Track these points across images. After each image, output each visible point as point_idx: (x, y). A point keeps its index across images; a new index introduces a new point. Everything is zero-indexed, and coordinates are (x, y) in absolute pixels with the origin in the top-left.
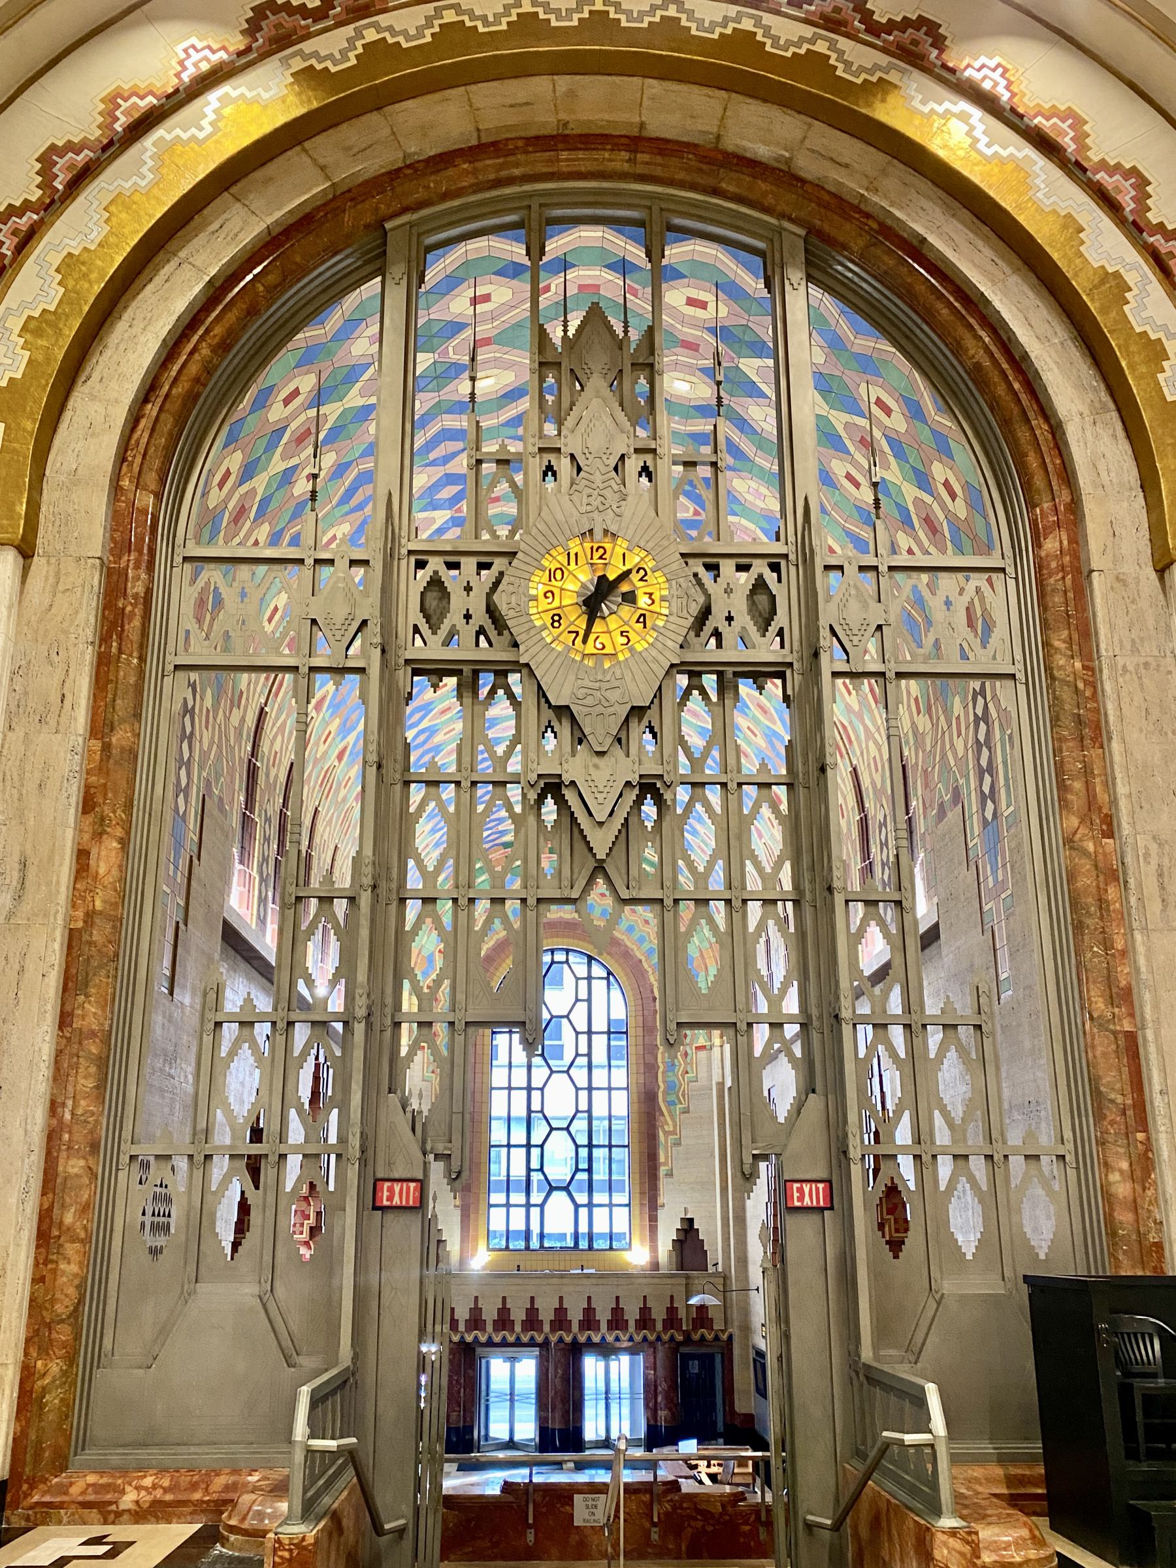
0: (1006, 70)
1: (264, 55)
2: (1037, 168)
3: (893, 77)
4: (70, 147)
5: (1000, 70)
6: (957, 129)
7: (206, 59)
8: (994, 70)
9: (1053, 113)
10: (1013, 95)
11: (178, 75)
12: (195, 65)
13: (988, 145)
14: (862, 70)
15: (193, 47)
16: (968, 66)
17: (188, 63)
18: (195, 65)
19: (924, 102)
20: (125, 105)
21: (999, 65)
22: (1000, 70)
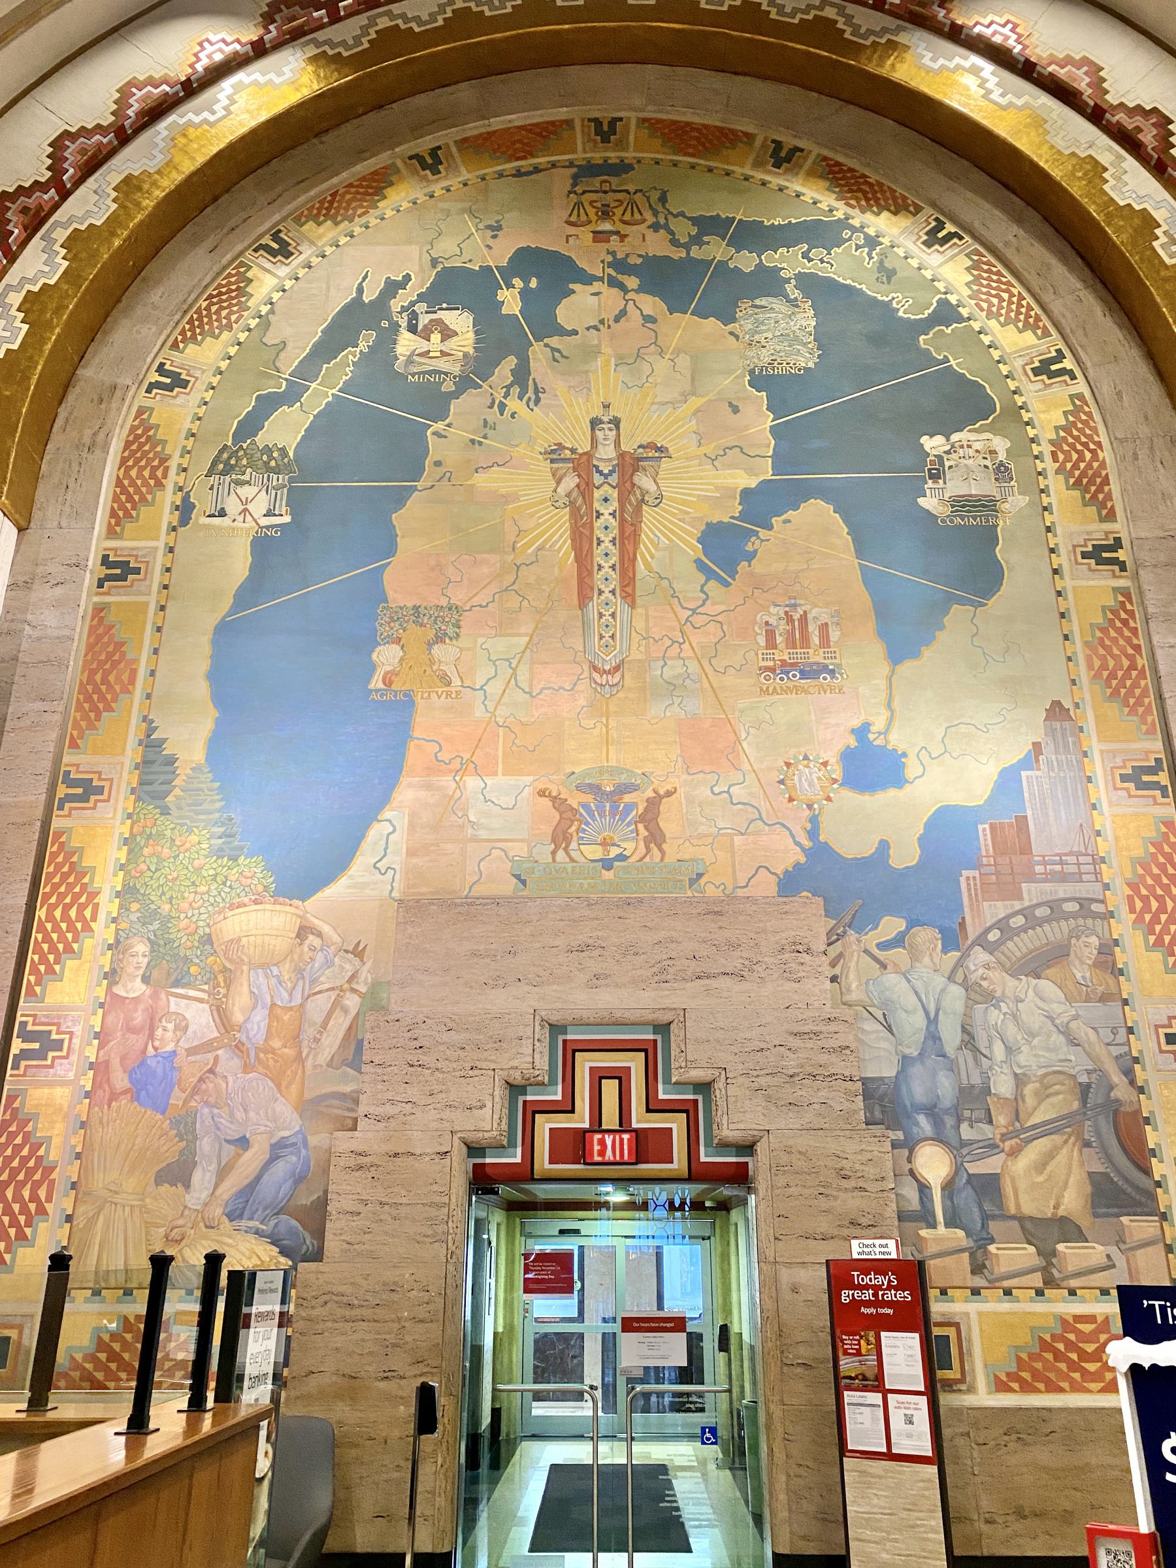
0: (1015, 26)
1: (278, 46)
2: (1054, 115)
3: (902, 38)
4: (83, 132)
5: (1010, 26)
6: (970, 81)
7: (221, 50)
8: (1004, 26)
9: (1068, 61)
10: (1025, 47)
11: (192, 66)
12: (209, 57)
13: (1002, 95)
14: (870, 32)
15: (208, 40)
16: (977, 23)
17: (202, 55)
18: (209, 57)
19: (934, 60)
20: (139, 94)
21: (1008, 22)
22: (1010, 26)
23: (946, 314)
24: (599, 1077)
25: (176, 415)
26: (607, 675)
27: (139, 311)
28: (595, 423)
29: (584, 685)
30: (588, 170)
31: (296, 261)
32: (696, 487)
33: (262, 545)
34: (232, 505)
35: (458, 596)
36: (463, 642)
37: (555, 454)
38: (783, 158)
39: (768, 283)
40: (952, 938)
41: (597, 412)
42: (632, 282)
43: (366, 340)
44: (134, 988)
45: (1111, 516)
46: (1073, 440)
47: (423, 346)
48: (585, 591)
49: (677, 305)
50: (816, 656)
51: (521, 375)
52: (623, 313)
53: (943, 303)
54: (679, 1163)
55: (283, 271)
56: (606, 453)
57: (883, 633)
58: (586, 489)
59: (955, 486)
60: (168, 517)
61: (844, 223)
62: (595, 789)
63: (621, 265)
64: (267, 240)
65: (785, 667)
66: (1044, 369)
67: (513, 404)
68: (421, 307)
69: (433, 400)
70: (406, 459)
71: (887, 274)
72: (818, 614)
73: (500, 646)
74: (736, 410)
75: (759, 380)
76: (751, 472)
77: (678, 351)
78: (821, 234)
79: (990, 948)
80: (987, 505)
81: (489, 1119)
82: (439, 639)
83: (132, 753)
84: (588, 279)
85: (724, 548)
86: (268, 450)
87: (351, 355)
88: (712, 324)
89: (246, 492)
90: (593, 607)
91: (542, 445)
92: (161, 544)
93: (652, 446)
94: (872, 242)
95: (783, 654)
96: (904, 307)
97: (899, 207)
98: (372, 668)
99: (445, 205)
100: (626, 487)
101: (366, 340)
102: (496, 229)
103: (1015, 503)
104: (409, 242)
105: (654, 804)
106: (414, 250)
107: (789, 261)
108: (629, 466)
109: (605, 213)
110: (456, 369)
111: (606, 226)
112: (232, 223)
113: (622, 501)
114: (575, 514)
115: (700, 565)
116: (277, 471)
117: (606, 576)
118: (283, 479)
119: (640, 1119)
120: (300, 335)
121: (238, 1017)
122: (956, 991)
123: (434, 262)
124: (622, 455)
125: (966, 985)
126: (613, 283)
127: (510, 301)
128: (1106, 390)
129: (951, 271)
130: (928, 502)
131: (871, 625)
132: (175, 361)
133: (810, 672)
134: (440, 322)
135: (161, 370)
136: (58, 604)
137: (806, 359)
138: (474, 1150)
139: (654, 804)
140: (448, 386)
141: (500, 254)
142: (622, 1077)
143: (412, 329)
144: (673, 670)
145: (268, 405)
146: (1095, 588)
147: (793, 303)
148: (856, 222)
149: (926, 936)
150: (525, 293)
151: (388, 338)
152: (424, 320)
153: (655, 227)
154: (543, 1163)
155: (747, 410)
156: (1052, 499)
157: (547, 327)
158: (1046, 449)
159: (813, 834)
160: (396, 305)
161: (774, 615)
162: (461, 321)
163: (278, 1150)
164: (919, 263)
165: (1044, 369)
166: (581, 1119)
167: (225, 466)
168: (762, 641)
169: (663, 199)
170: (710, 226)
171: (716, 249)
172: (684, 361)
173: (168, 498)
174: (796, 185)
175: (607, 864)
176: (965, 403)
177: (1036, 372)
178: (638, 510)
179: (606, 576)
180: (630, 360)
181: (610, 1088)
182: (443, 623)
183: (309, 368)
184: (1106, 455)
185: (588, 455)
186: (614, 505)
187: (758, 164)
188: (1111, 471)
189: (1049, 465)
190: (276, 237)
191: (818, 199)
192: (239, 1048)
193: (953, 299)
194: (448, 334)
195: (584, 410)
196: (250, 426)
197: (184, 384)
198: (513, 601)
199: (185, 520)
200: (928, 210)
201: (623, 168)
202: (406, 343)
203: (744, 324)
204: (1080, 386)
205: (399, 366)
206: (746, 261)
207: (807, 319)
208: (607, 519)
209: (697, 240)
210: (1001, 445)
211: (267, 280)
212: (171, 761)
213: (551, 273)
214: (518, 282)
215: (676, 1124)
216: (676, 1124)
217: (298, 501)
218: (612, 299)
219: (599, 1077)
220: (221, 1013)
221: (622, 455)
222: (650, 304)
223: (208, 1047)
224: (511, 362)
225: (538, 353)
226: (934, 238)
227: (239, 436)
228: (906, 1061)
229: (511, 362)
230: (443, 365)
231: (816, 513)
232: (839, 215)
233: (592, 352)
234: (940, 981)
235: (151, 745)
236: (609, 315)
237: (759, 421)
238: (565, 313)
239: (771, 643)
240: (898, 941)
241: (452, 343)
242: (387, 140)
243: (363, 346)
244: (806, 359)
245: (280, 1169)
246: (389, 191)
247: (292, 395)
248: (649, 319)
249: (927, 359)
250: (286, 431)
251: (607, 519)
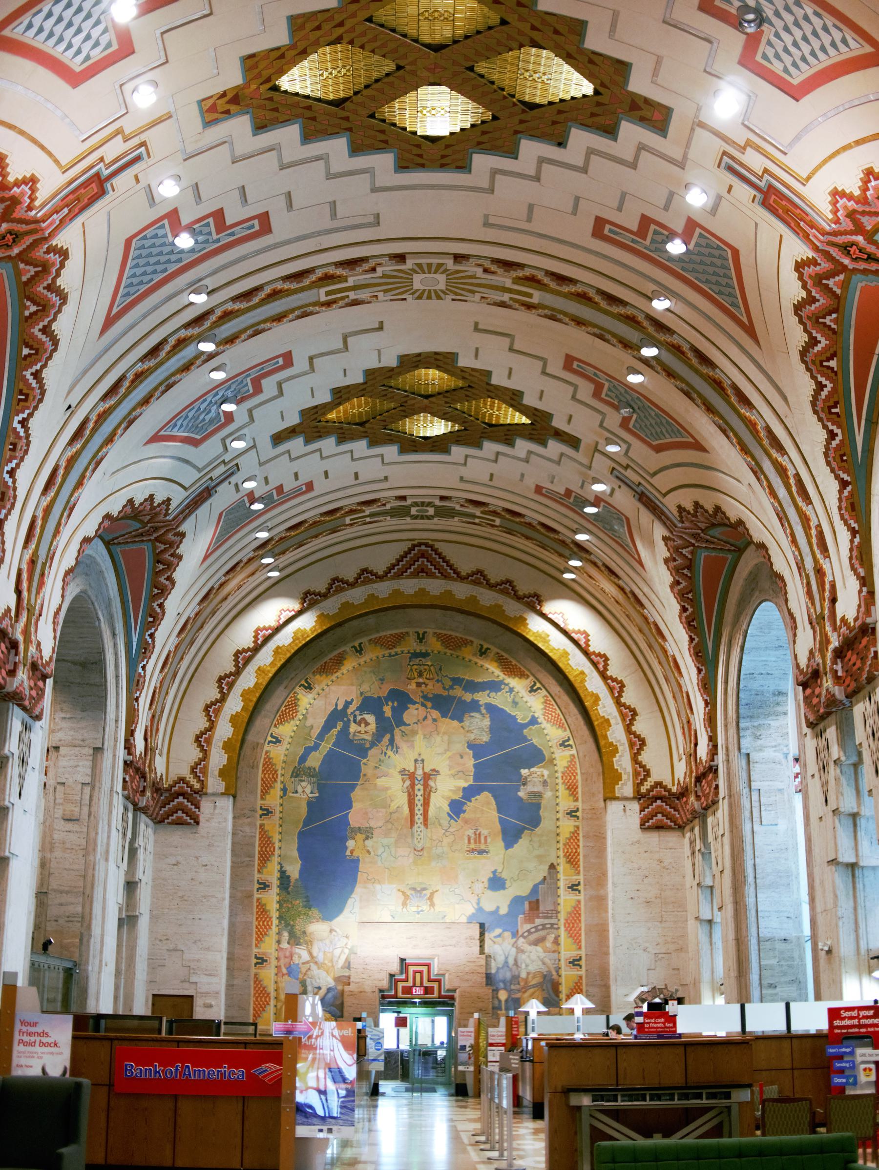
23: (534, 721)
24: (415, 972)
25: (278, 753)
26: (419, 852)
27: (263, 713)
28: (416, 761)
29: (412, 855)
30: (415, 655)
31: (314, 692)
32: (447, 787)
33: (310, 804)
34: (300, 790)
35: (372, 824)
36: (375, 839)
37: (403, 772)
38: (483, 653)
39: (474, 706)
40: (515, 934)
41: (416, 757)
42: (429, 704)
43: (340, 725)
44: (285, 945)
45: (577, 800)
46: (570, 771)
47: (359, 729)
48: (412, 823)
49: (444, 715)
50: (483, 847)
51: (392, 741)
52: (425, 718)
53: (533, 716)
54: (436, 995)
55: (310, 696)
56: (420, 772)
57: (504, 840)
58: (413, 785)
59: (530, 788)
60: (279, 793)
61: (502, 682)
62: (414, 889)
63: (425, 697)
64: (303, 682)
65: (473, 850)
66: (564, 744)
67: (389, 753)
68: (357, 713)
69: (362, 750)
70: (354, 773)
71: (515, 703)
72: (485, 832)
73: (386, 841)
74: (462, 757)
75: (471, 746)
76: (466, 781)
77: (444, 733)
78: (495, 686)
79: (525, 938)
80: (539, 795)
81: (385, 984)
82: (367, 838)
83: (277, 875)
84: (414, 703)
85: (456, 808)
86: (309, 768)
87: (334, 732)
88: (455, 723)
89: (304, 784)
90: (415, 827)
91: (399, 769)
92: (279, 801)
93: (434, 770)
94: (511, 690)
95: (473, 846)
96: (521, 717)
97: (522, 675)
98: (346, 848)
99: (365, 669)
100: (426, 786)
101: (340, 725)
102: (382, 680)
103: (548, 794)
104: (352, 685)
105: (432, 894)
106: (354, 688)
107: (483, 698)
108: (427, 777)
109: (420, 675)
110: (369, 738)
111: (421, 680)
112: (292, 675)
113: (425, 790)
114: (409, 795)
115: (449, 815)
116: (313, 776)
117: (419, 818)
118: (315, 779)
119: (426, 984)
120: (318, 722)
121: (315, 954)
122: (514, 950)
123: (362, 694)
124: (425, 773)
125: (517, 948)
126: (423, 705)
127: (388, 711)
128: (581, 754)
129: (535, 704)
130: (521, 794)
131: (500, 837)
132: (275, 731)
133: (481, 852)
134: (363, 719)
135: (272, 736)
136: (250, 824)
137: (486, 738)
138: (381, 991)
139: (432, 894)
140: (368, 745)
141: (384, 693)
142: (421, 972)
143: (355, 721)
144: (439, 850)
145: (308, 751)
146: (567, 826)
147: (483, 715)
148: (506, 681)
149: (507, 934)
150: (393, 708)
151: (346, 726)
152: (359, 718)
153: (438, 681)
154: (400, 994)
155: (465, 757)
156: (559, 794)
157: (401, 723)
158: (559, 775)
159: (478, 904)
160: (349, 711)
161: (470, 832)
162: (370, 718)
163: (329, 990)
164: (525, 700)
165: (564, 744)
166: (410, 983)
167: (297, 774)
168: (466, 841)
169: (440, 669)
170: (457, 681)
171: (458, 692)
172: (446, 738)
173: (278, 786)
174: (487, 665)
175: (418, 913)
176: (535, 757)
177: (561, 745)
178: (429, 795)
179: (419, 818)
180: (428, 737)
181: (418, 975)
182: (368, 833)
183: (321, 736)
184: (579, 777)
185: (413, 773)
186: (422, 792)
187: (474, 655)
188: (580, 784)
189: (560, 781)
190: (306, 682)
191: (493, 670)
192: (316, 963)
193: (536, 715)
194: (367, 724)
195: (412, 755)
196: (303, 759)
197: (280, 742)
198: (390, 826)
199: (285, 794)
200: (531, 678)
201: (425, 655)
202: (353, 728)
203: (466, 723)
204: (574, 752)
205: (351, 737)
206: (468, 697)
207: (487, 722)
208: (419, 797)
209: (451, 687)
210: (546, 773)
211: (305, 699)
212: (289, 877)
213: (401, 700)
214: (390, 703)
215: (436, 985)
216: (436, 985)
217: (321, 788)
218: (422, 711)
219: (415, 972)
220: (310, 954)
221: (425, 773)
222: (435, 714)
223: (307, 962)
224: (388, 736)
225: (397, 732)
226: (532, 690)
227: (300, 763)
228: (498, 969)
229: (388, 736)
230: (365, 736)
231: (486, 797)
232: (501, 678)
233: (414, 733)
234: (510, 947)
235: (282, 872)
236: (421, 718)
237: (470, 762)
238: (407, 717)
239: (469, 842)
240: (499, 936)
241: (369, 728)
242: (343, 641)
243: (339, 728)
244: (486, 738)
245: (330, 995)
246: (345, 662)
247: (316, 747)
248: (435, 720)
249: (525, 739)
250: (315, 761)
251: (419, 797)
